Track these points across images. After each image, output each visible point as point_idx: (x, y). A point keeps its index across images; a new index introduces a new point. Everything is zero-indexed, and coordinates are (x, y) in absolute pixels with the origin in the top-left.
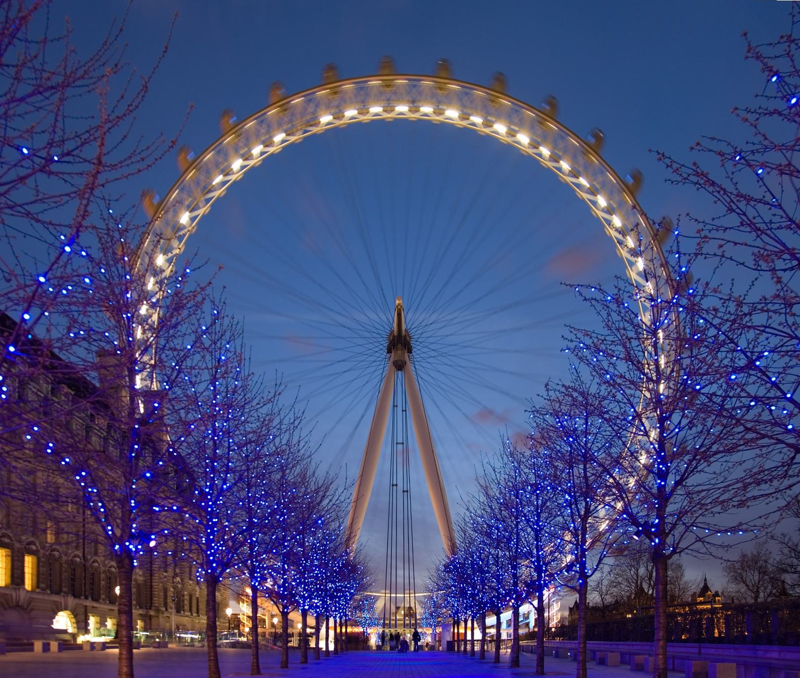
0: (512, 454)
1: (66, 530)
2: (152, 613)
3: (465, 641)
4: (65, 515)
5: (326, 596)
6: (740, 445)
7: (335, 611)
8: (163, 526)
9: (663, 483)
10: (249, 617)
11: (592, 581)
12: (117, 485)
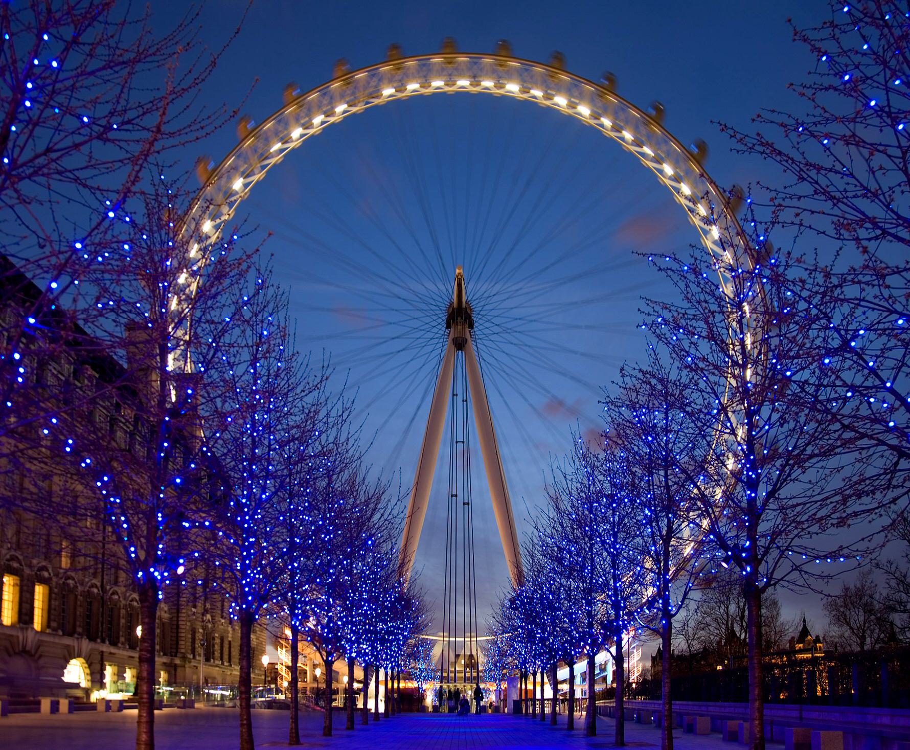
0: (584, 457)
1: (83, 551)
2: (177, 661)
3: (534, 699)
4: (82, 531)
5: (376, 639)
6: (838, 447)
7: (386, 659)
8: (193, 546)
9: (753, 495)
10: (287, 667)
11: (677, 622)
12: (143, 494)
